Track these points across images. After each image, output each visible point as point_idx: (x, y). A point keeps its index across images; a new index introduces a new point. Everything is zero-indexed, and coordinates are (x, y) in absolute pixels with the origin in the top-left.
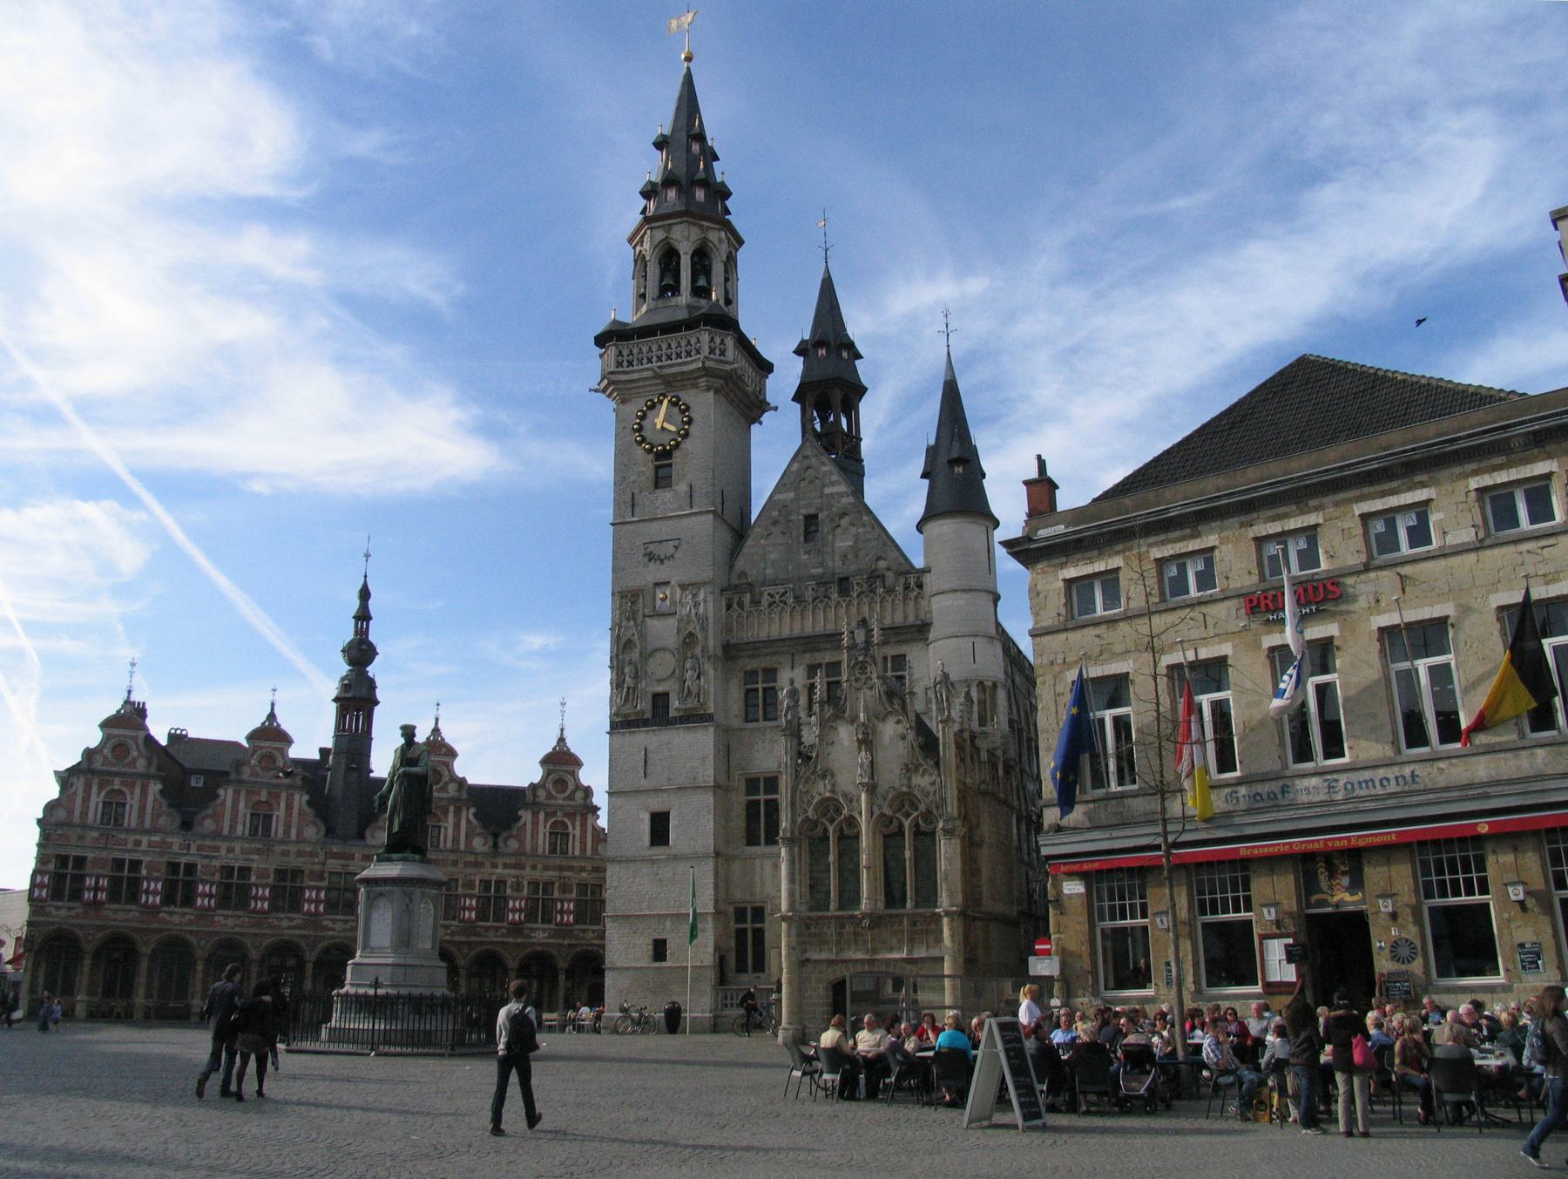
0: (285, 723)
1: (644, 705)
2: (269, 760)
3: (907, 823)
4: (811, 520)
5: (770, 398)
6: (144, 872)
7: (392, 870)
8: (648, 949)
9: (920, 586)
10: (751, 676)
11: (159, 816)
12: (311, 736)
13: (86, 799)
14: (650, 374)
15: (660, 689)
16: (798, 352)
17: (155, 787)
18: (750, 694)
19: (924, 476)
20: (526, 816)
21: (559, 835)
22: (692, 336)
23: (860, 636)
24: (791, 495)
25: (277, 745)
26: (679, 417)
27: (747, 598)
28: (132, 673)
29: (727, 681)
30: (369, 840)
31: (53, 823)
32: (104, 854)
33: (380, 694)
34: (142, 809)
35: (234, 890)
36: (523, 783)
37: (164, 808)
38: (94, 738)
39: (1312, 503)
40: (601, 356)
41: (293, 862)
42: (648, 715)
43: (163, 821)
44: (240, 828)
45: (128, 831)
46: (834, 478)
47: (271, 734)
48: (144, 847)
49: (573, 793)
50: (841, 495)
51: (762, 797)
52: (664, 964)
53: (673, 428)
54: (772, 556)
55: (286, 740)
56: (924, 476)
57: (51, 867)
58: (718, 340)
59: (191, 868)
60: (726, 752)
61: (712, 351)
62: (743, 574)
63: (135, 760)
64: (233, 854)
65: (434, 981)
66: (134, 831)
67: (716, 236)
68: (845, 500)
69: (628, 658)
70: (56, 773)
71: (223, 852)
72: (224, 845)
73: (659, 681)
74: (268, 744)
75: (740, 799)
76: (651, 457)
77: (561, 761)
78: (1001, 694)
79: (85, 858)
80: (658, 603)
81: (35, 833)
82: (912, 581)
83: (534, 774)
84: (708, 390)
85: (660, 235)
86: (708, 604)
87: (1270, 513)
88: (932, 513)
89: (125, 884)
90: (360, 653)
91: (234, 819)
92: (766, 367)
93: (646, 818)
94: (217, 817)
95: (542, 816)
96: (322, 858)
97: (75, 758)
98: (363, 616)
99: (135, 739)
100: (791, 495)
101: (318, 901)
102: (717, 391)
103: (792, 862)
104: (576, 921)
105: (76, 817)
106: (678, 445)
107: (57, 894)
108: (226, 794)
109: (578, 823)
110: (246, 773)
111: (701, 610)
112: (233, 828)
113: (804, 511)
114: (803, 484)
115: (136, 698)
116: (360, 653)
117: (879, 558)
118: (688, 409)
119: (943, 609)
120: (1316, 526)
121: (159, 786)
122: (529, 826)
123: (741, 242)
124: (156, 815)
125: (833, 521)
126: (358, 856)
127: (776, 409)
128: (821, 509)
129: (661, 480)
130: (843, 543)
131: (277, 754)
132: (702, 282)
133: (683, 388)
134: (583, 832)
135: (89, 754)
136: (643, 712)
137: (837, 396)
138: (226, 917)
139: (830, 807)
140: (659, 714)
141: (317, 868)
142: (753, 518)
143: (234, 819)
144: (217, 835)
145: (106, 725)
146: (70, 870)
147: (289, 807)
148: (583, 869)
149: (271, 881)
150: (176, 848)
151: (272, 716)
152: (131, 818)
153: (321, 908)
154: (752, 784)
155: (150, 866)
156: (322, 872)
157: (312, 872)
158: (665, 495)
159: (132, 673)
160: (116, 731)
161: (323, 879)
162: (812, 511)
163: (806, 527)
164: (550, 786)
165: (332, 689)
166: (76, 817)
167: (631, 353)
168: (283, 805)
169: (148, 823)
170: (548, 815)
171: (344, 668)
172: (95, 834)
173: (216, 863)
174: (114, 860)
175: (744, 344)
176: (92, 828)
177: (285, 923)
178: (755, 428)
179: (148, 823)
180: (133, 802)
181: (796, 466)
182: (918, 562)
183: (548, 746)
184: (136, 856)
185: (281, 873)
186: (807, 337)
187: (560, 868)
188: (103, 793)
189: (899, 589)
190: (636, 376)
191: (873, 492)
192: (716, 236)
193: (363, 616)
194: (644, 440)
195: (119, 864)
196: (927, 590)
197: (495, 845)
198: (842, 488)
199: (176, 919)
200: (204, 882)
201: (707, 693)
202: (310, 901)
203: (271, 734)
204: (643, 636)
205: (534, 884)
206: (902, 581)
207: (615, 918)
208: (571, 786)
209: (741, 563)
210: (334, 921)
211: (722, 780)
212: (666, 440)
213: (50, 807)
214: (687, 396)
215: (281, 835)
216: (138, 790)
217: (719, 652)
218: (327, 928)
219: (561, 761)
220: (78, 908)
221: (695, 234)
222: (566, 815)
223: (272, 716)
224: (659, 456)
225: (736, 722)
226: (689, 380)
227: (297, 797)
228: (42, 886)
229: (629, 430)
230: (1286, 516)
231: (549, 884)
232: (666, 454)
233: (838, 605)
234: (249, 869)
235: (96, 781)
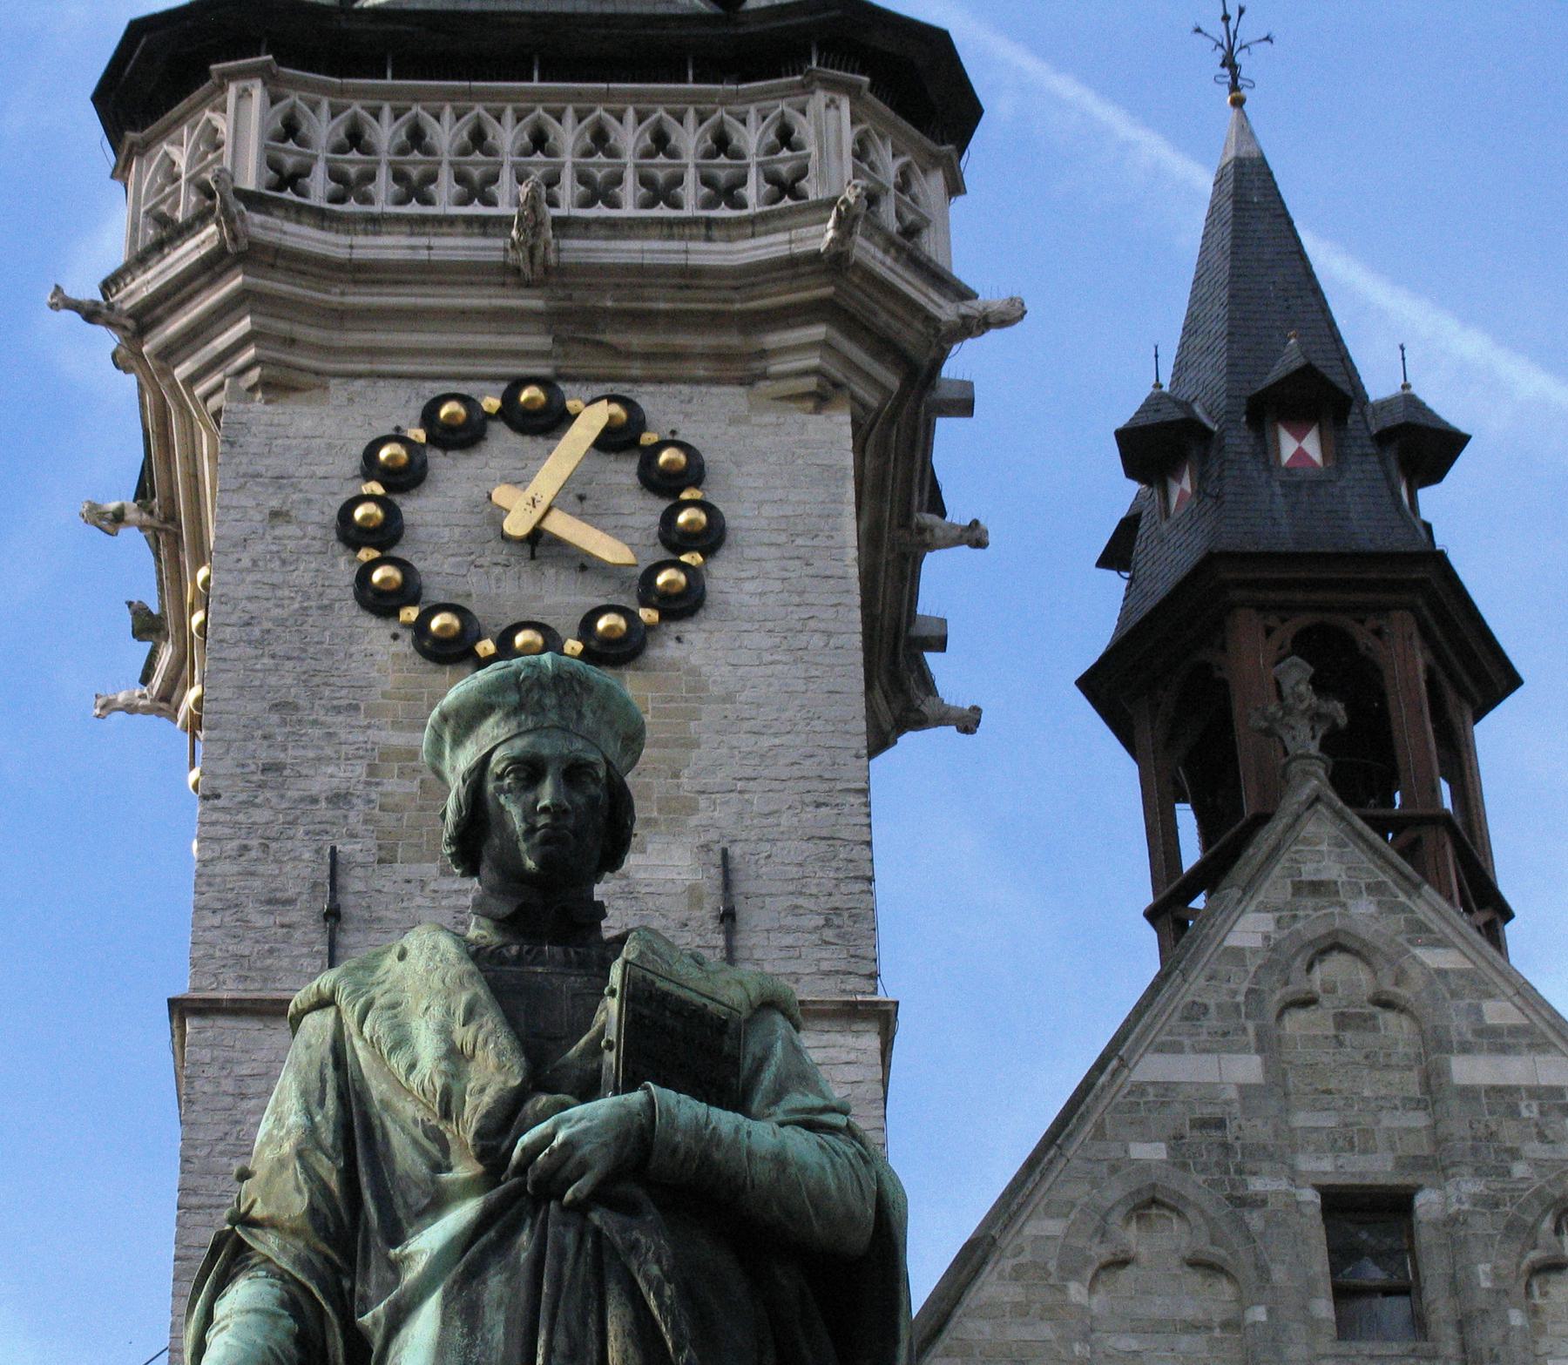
4: (1367, 1219)
14: (490, 249)
26: (647, 511)
58: (889, 167)
84: (821, 400)
100: (1247, 1068)
113: (1325, 1167)
114: (1296, 1023)
118: (694, 472)
128: (1437, 1165)
133: (667, 367)
137: (1406, 662)
163: (1341, 1254)
167: (355, 138)
190: (391, 246)
194: (408, 591)
212: (561, 599)
226: (718, 327)
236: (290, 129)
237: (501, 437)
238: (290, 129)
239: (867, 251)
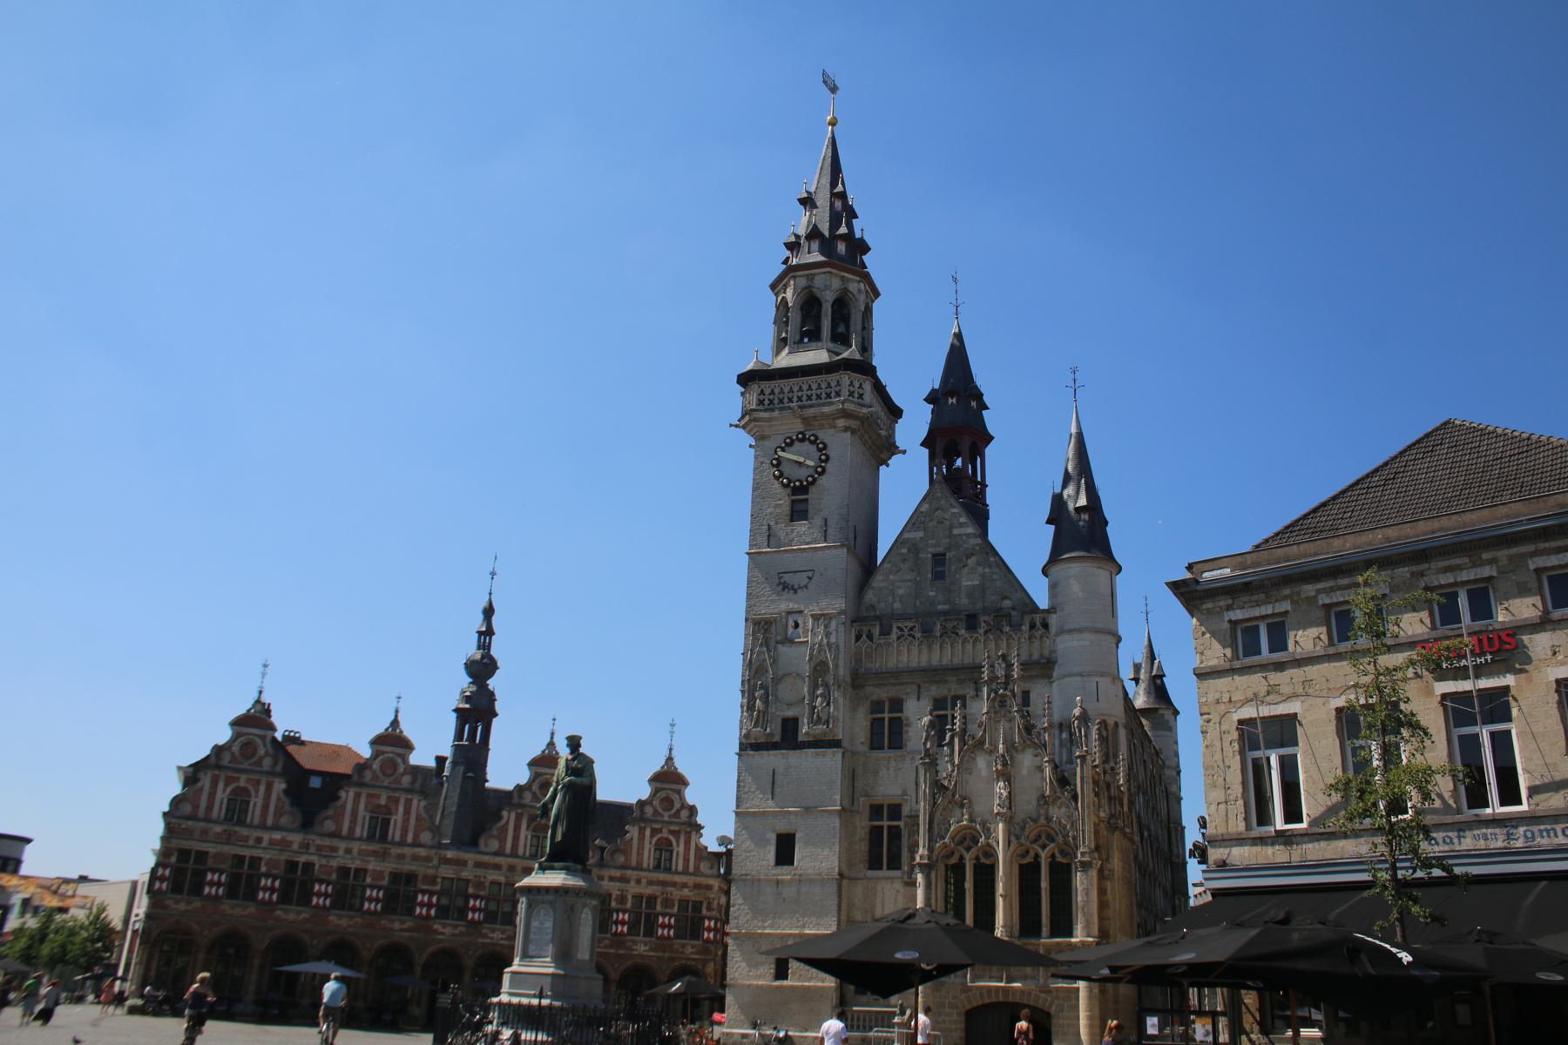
0: (408, 730)
1: (774, 730)
2: (390, 767)
3: (1044, 856)
5: (900, 441)
6: (263, 869)
7: (555, 878)
8: (770, 969)
9: (1046, 626)
10: (877, 706)
11: (281, 815)
12: (432, 743)
13: (212, 795)
15: (790, 713)
16: (928, 400)
17: (280, 786)
18: (876, 724)
19: (1049, 522)
20: (633, 832)
21: (664, 847)
22: (832, 378)
23: (1000, 672)
24: (921, 534)
25: (399, 750)
27: (876, 631)
28: (264, 675)
29: (854, 709)
30: (482, 846)
31: (176, 816)
32: (226, 849)
33: (498, 706)
34: (266, 807)
35: (348, 888)
36: (633, 801)
37: (287, 807)
38: (224, 735)
39: (1485, 556)
40: (743, 394)
41: (407, 867)
42: (777, 738)
43: (284, 820)
44: (358, 832)
45: (251, 826)
46: (962, 520)
47: (393, 741)
48: (265, 844)
49: (678, 812)
50: (968, 535)
51: (885, 823)
52: (785, 983)
53: (811, 463)
54: (901, 592)
55: (407, 746)
56: (1049, 522)
57: (173, 859)
58: (857, 385)
59: (309, 866)
60: (851, 776)
61: (851, 394)
62: (872, 607)
63: (261, 759)
64: (350, 855)
65: (592, 991)
66: (257, 827)
67: (855, 286)
68: (973, 541)
69: (760, 682)
70: (180, 768)
71: (341, 852)
72: (342, 845)
73: (790, 705)
74: (389, 749)
75: (862, 824)
76: (789, 491)
77: (668, 780)
78: (1122, 733)
79: (207, 853)
80: (790, 630)
81: (159, 827)
82: (1038, 619)
83: (645, 792)
85: (803, 282)
86: (840, 635)
87: (1442, 564)
88: (1055, 557)
89: (242, 882)
90: (482, 669)
91: (353, 821)
92: (896, 413)
93: (773, 837)
94: (338, 818)
95: (648, 832)
96: (436, 862)
97: (203, 751)
98: (487, 633)
99: (263, 738)
100: (921, 534)
101: (430, 905)
102: (853, 432)
103: (928, 886)
104: (677, 936)
105: (201, 813)
106: (815, 480)
107: (176, 888)
108: (348, 795)
109: (682, 840)
110: (368, 776)
111: (833, 639)
112: (352, 829)
113: (932, 550)
115: (265, 699)
116: (482, 669)
117: (1005, 598)
118: (825, 447)
119: (1069, 647)
120: (1490, 579)
121: (283, 786)
122: (635, 841)
123: (877, 294)
124: (279, 813)
125: (960, 560)
126: (471, 863)
127: (904, 452)
128: (949, 549)
129: (798, 512)
130: (968, 581)
131: (399, 760)
132: (841, 329)
133: (822, 427)
134: (687, 849)
135: (218, 750)
136: (771, 734)
138: (340, 917)
139: (968, 838)
140: (789, 737)
141: (430, 872)
142: (881, 554)
143: (353, 821)
144: (336, 835)
145: (238, 723)
146: (191, 865)
147: (407, 812)
148: (685, 885)
149: (385, 882)
150: (295, 846)
151: (395, 723)
152: (254, 815)
153: (433, 912)
154: (876, 811)
155: (270, 863)
156: (435, 877)
157: (425, 877)
158: (802, 527)
159: (264, 675)
160: (245, 730)
161: (435, 883)
162: (940, 550)
164: (656, 803)
165: (455, 701)
166: (201, 813)
168: (401, 809)
169: (270, 821)
170: (654, 832)
171: (464, 681)
172: (218, 829)
173: (334, 863)
174: (236, 856)
175: (880, 389)
176: (216, 822)
177: (397, 926)
178: (883, 468)
179: (270, 821)
180: (257, 801)
181: (925, 507)
182: (1043, 602)
183: (657, 765)
184: (257, 853)
185: (396, 877)
186: (937, 386)
187: (663, 883)
188: (229, 789)
189: (1025, 628)
191: (997, 535)
192: (853, 287)
193: (487, 633)
194: (781, 475)
195: (240, 859)
196: (1053, 629)
197: (602, 858)
198: (970, 530)
199: (291, 917)
200: (321, 882)
201: (836, 720)
202: (422, 905)
203: (393, 741)
204: (775, 662)
205: (638, 898)
206: (1027, 619)
207: (737, 937)
208: (677, 805)
209: (870, 596)
210: (444, 926)
211: (847, 803)
212: (802, 473)
213: (176, 802)
214: (825, 435)
215: (397, 838)
216: (262, 788)
217: (849, 680)
218: (436, 932)
219: (668, 780)
220: (197, 904)
221: (836, 283)
222: (671, 832)
223: (395, 723)
224: (795, 491)
225: (865, 748)
227: (415, 802)
228: (162, 879)
229: (767, 466)
230: (1459, 568)
231: (651, 900)
232: (803, 489)
233: (965, 641)
234: (366, 871)
235: (222, 777)
236: (762, 392)
237: (797, 444)
238: (762, 392)
239: (849, 406)
